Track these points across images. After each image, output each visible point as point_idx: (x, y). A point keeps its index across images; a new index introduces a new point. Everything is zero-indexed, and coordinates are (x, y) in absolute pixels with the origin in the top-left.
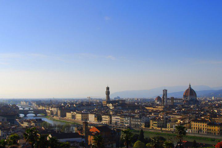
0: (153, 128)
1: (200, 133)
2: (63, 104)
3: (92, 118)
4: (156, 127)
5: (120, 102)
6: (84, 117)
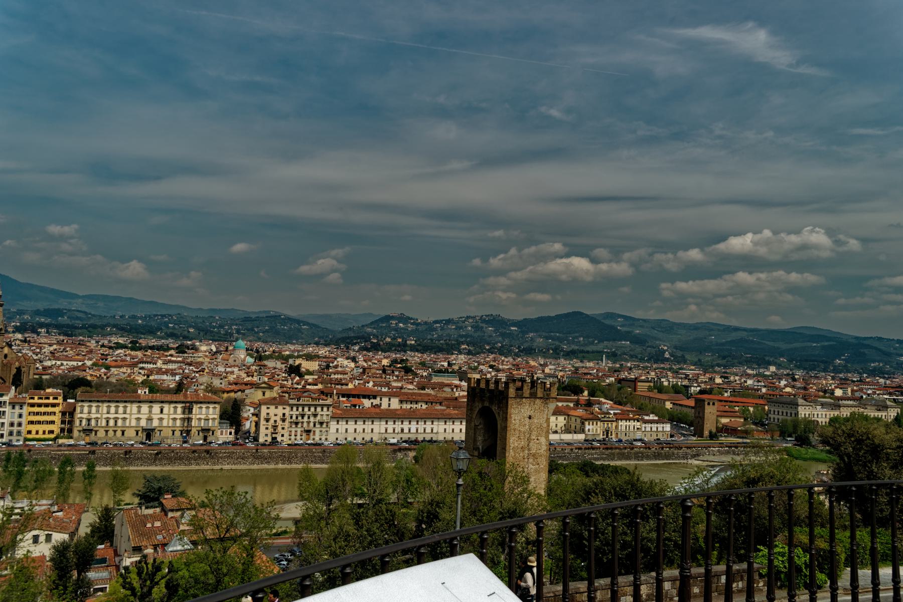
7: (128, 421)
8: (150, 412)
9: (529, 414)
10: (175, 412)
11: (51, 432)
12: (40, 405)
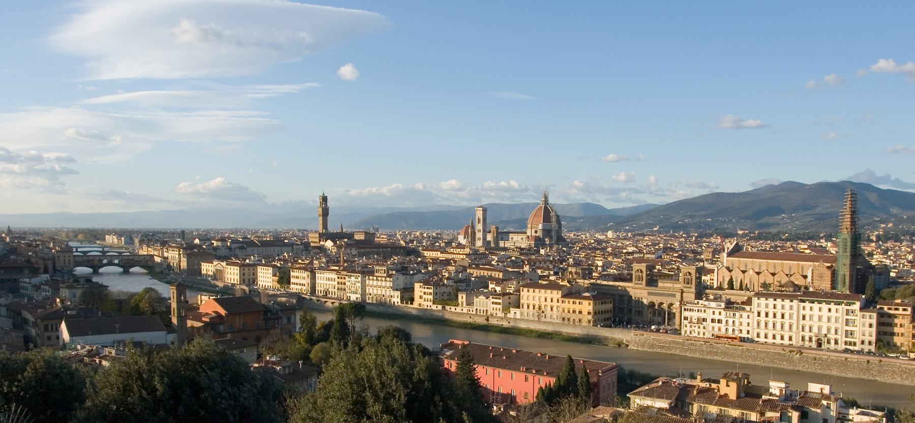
0: (420, 305)
1: (543, 319)
2: (197, 241)
3: (266, 278)
4: (431, 303)
5: (359, 237)
6: (246, 274)
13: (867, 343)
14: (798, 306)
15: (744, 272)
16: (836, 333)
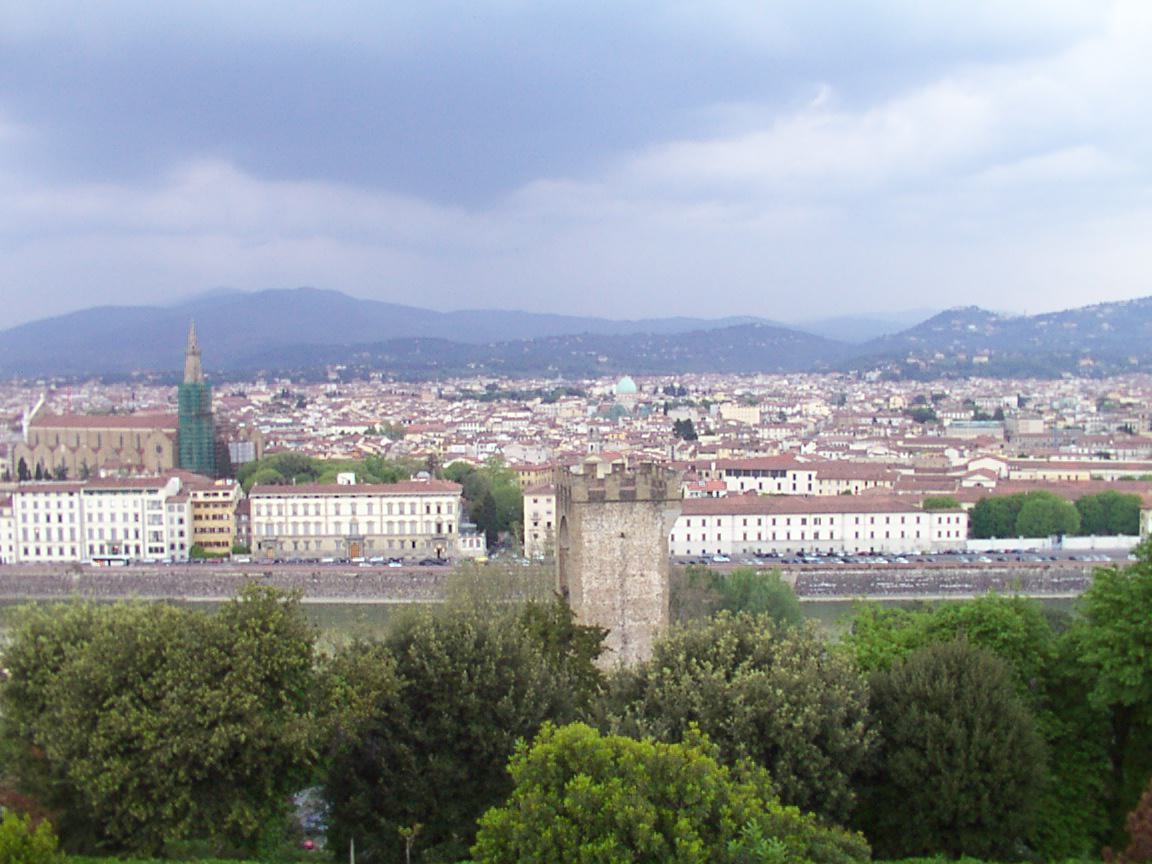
7: (323, 526)
8: (354, 513)
9: (620, 530)
10: (390, 512)
11: (226, 544)
12: (207, 505)
13: (177, 547)
14: (81, 501)
15: (52, 449)
16: (137, 536)
